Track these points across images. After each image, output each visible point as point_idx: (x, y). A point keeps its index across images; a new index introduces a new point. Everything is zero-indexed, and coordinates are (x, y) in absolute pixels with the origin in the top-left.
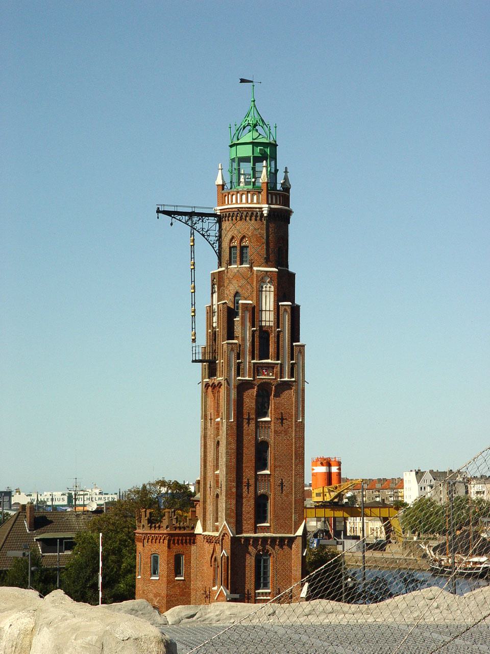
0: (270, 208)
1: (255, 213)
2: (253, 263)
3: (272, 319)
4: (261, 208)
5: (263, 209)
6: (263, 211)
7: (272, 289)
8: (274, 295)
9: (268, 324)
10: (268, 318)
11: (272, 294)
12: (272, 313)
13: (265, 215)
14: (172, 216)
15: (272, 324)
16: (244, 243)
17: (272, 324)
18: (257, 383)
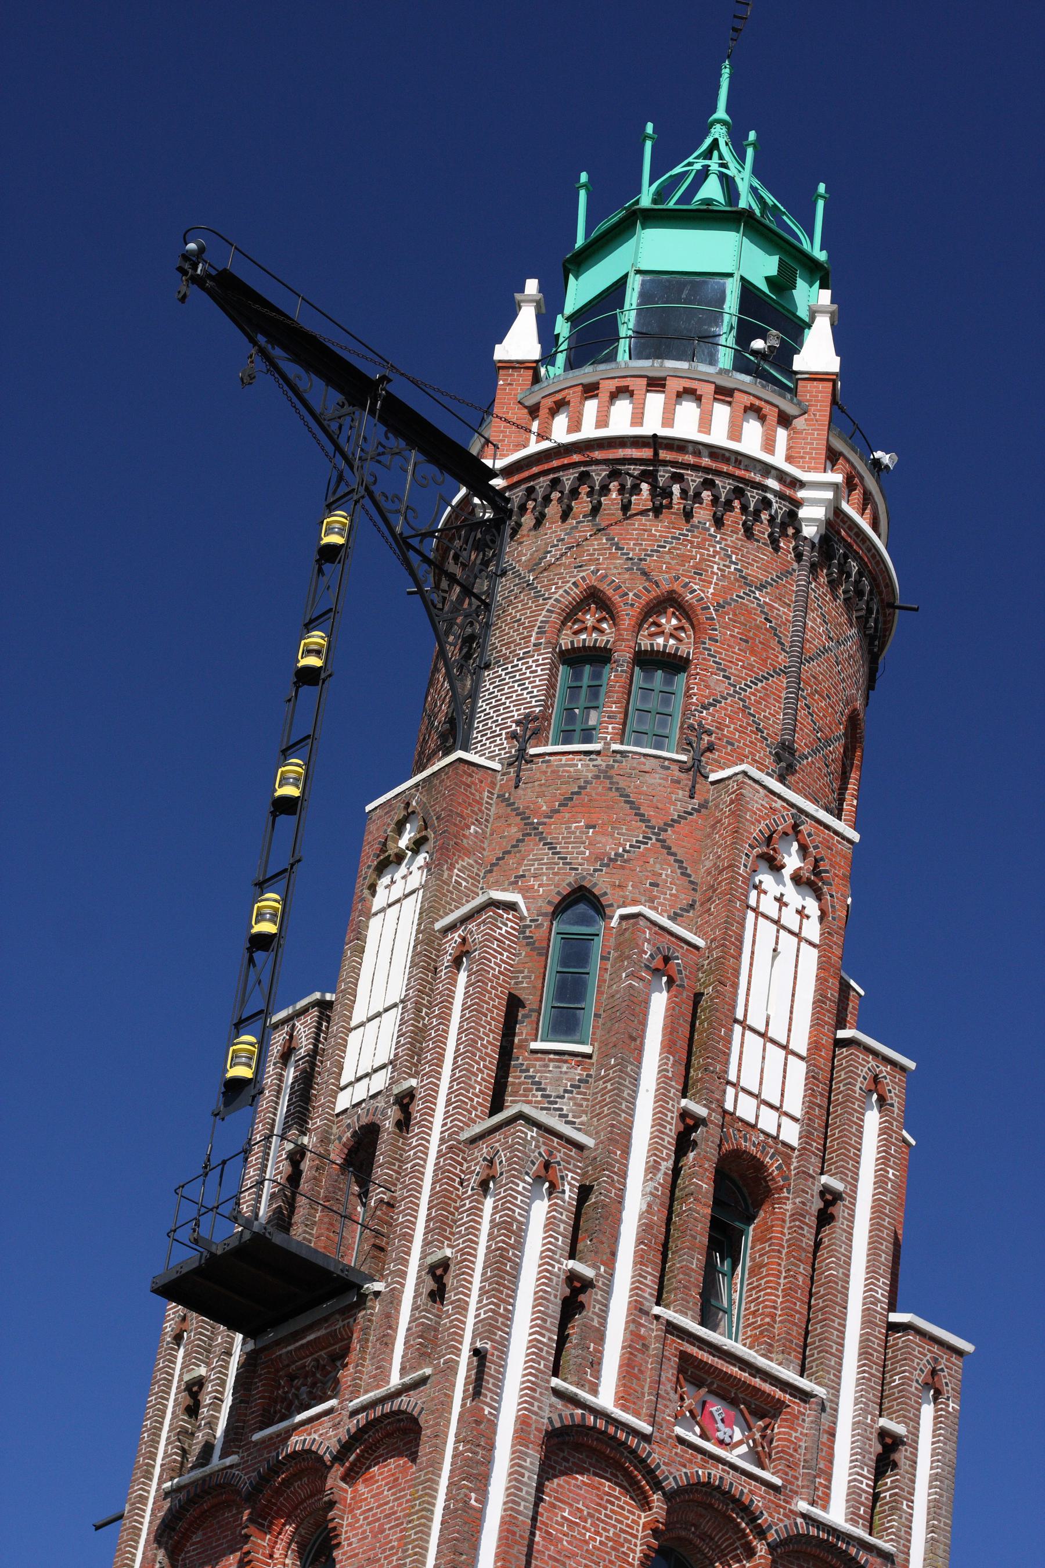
0: (838, 512)
1: (753, 497)
2: (710, 748)
3: (795, 1105)
4: (797, 484)
5: (801, 494)
6: (798, 504)
7: (813, 930)
8: (823, 966)
9: (768, 1121)
10: (768, 1085)
11: (810, 958)
12: (798, 1070)
13: (809, 531)
14: (261, 339)
15: (791, 1134)
16: (660, 640)
17: (791, 1134)
18: (676, 1471)
